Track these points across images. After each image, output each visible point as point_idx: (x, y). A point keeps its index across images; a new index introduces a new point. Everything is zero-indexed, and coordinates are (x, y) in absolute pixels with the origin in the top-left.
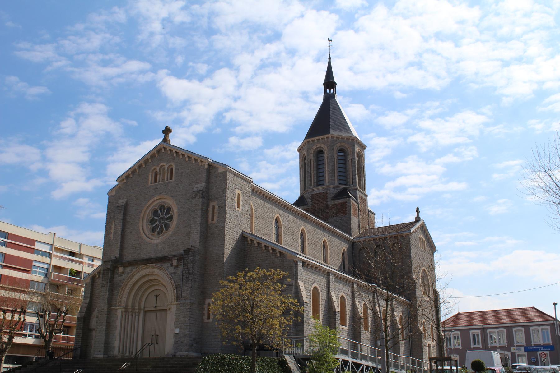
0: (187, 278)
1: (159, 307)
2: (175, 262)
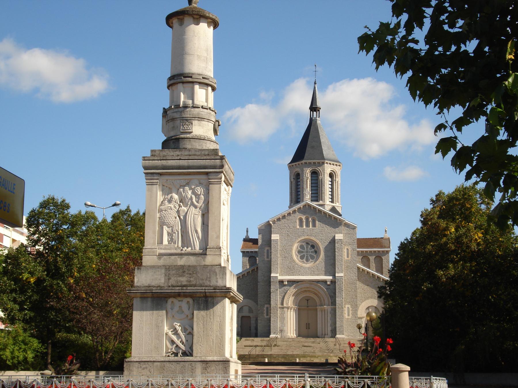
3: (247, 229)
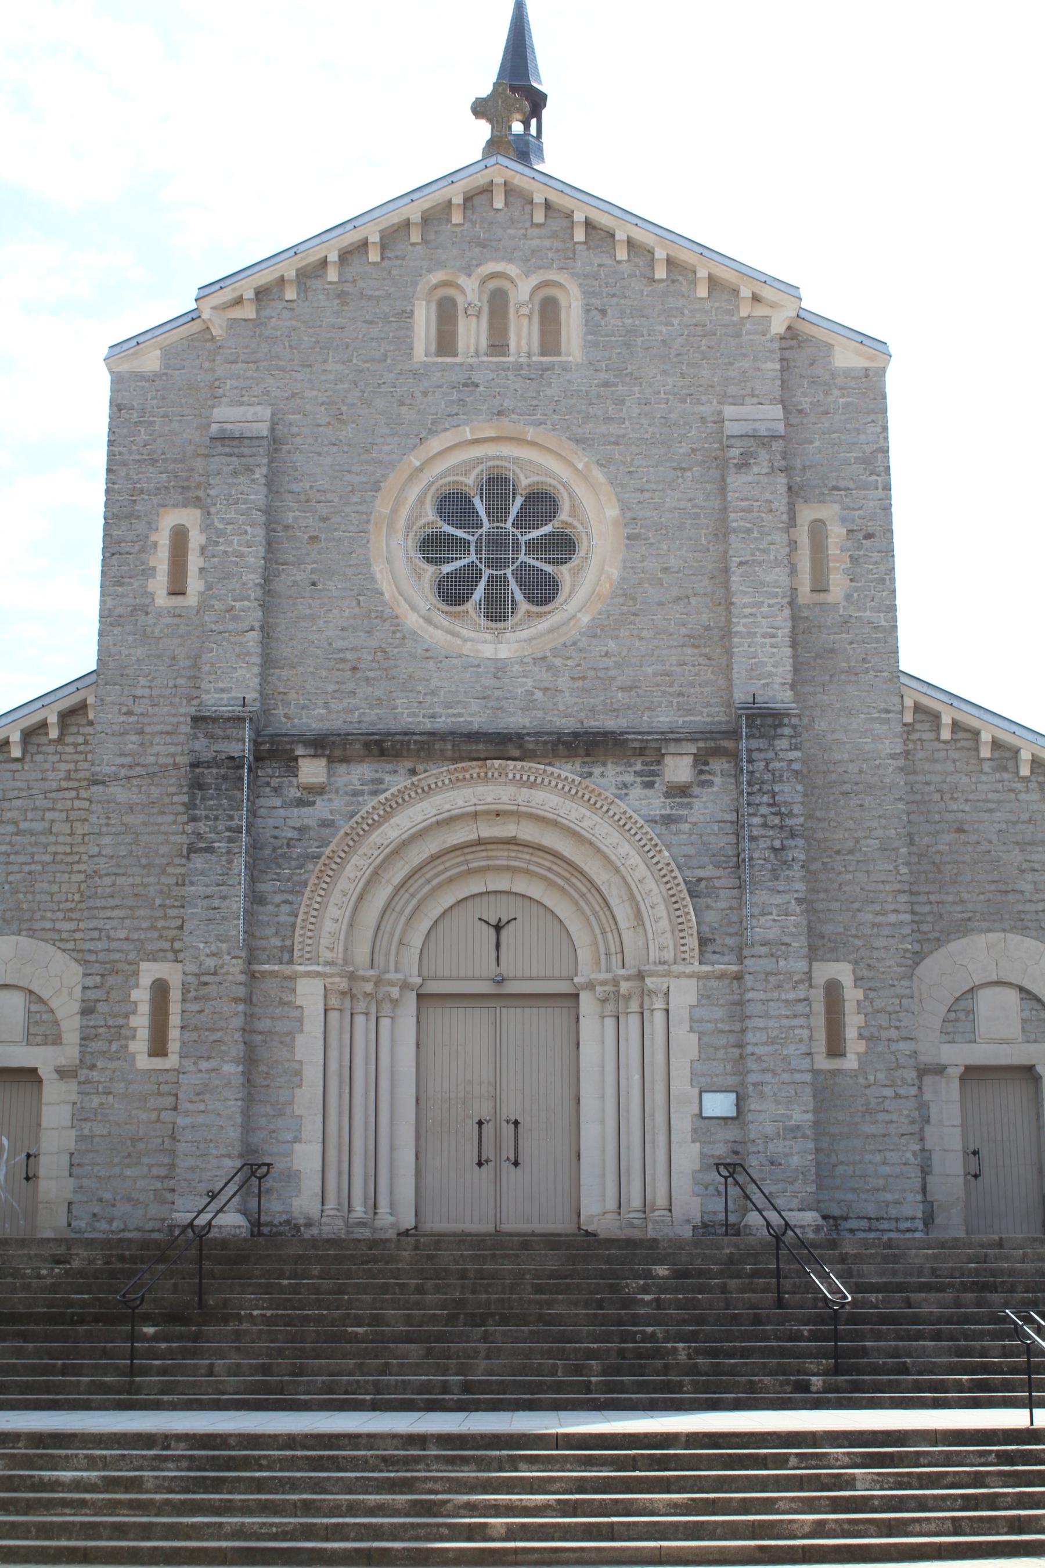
0: (773, 849)
1: (515, 979)
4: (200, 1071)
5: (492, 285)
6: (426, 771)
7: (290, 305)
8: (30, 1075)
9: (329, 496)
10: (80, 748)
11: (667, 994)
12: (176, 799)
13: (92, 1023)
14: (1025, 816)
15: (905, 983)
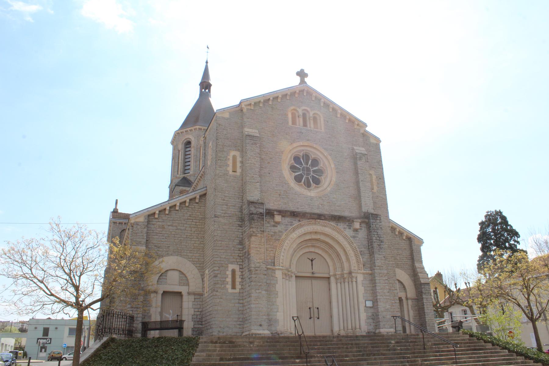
0: (378, 245)
2: (357, 225)
3: (117, 201)
4: (256, 293)
5: (304, 112)
6: (302, 221)
7: (261, 108)
8: (179, 294)
9: (272, 153)
10: (193, 209)
11: (356, 277)
12: (236, 223)
13: (216, 280)
14: (397, 243)
15: (395, 277)
